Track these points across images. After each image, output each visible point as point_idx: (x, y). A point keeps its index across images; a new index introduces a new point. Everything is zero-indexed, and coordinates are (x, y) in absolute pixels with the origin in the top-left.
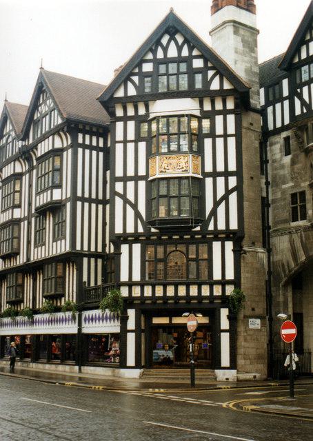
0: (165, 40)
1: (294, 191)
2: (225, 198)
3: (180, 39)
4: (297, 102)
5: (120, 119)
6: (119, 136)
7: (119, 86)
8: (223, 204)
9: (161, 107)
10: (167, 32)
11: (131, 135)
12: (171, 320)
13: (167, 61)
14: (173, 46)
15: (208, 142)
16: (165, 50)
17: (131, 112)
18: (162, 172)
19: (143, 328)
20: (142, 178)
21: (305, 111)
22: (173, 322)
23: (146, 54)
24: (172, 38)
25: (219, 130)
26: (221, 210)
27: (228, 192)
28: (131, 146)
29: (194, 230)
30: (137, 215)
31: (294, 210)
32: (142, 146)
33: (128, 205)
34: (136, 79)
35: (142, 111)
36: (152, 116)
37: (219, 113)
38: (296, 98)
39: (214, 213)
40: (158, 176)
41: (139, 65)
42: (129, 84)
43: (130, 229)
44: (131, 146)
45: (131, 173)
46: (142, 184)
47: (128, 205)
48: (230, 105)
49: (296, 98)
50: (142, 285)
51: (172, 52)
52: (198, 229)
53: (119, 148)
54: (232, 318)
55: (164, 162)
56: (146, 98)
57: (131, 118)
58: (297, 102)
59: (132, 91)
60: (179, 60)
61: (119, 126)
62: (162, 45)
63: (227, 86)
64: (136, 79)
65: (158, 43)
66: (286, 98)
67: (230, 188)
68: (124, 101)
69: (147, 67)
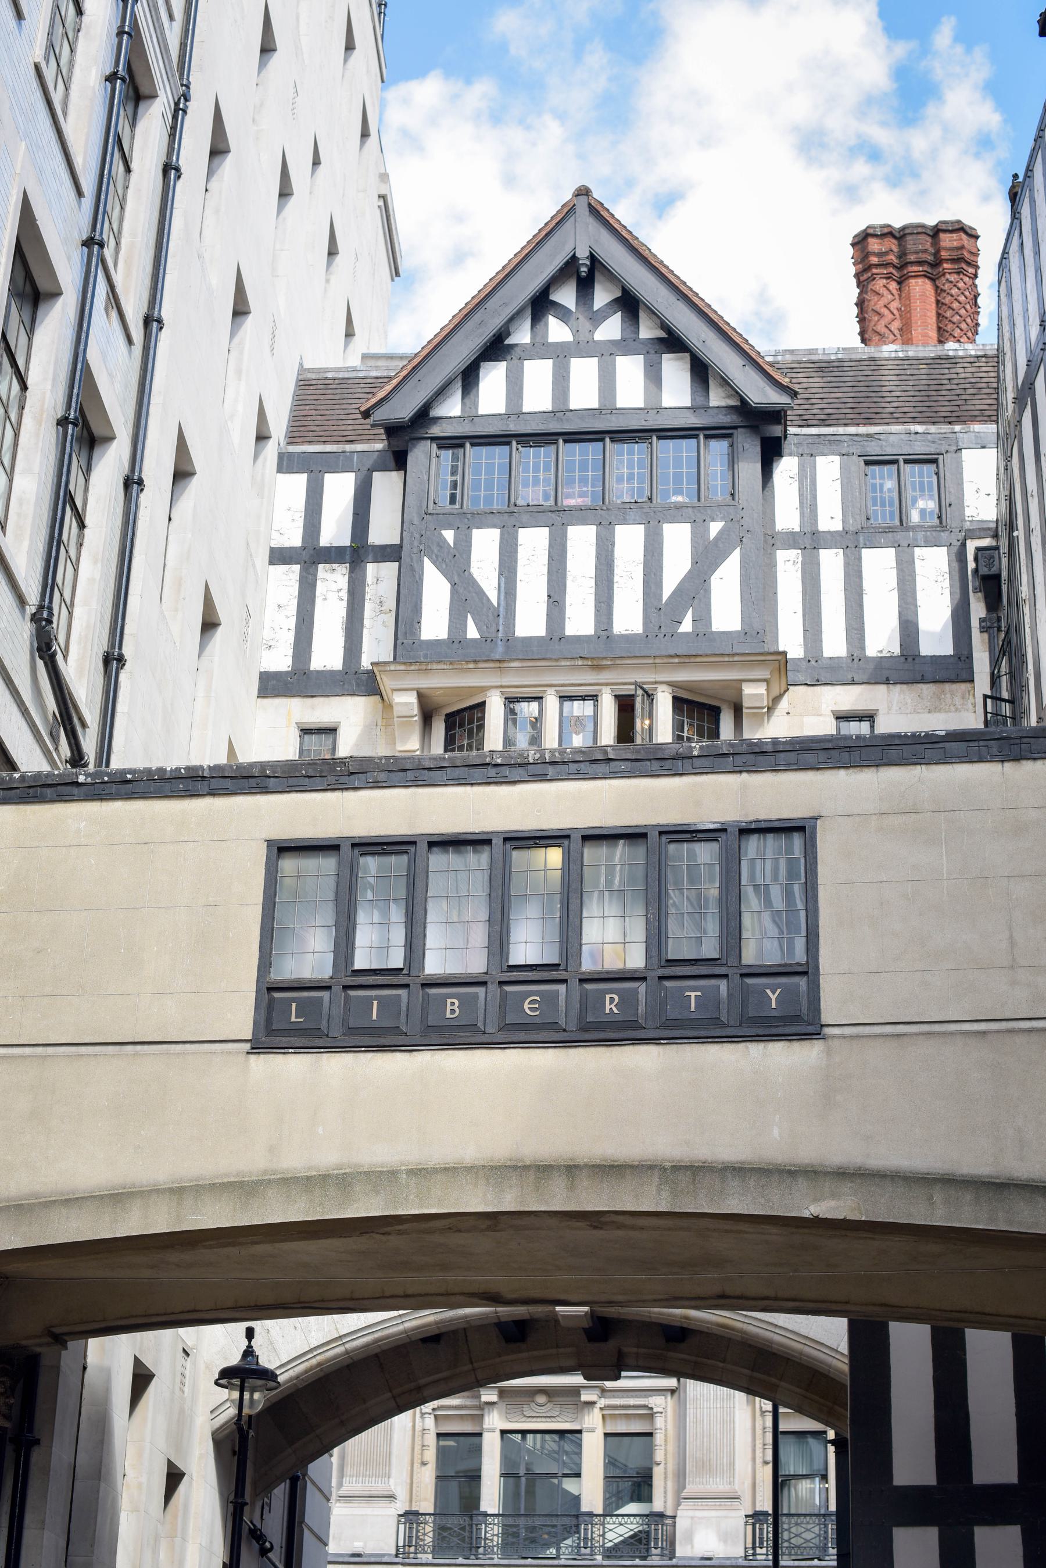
4: (436, 590)
21: (472, 632)
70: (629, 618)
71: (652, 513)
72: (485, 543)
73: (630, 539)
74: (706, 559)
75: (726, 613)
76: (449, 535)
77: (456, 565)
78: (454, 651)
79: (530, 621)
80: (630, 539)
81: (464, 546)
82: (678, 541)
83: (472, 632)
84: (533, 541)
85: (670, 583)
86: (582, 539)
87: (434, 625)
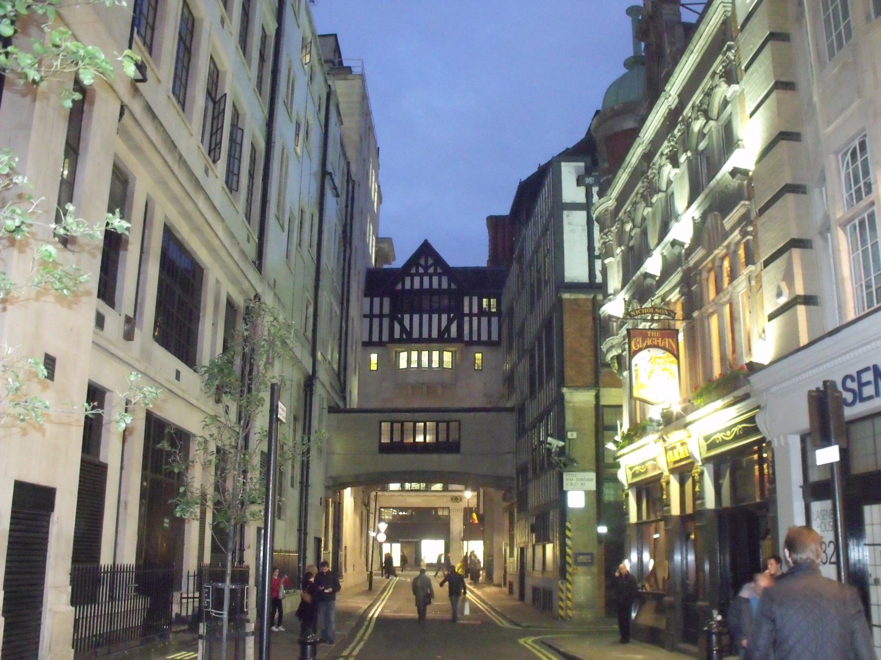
4: (397, 328)
21: (404, 337)
58: (397, 328)
71: (440, 312)
72: (407, 317)
73: (435, 317)
79: (416, 335)
80: (435, 317)
82: (444, 317)
83: (404, 337)
84: (416, 317)
85: (443, 328)
86: (426, 317)
87: (397, 335)
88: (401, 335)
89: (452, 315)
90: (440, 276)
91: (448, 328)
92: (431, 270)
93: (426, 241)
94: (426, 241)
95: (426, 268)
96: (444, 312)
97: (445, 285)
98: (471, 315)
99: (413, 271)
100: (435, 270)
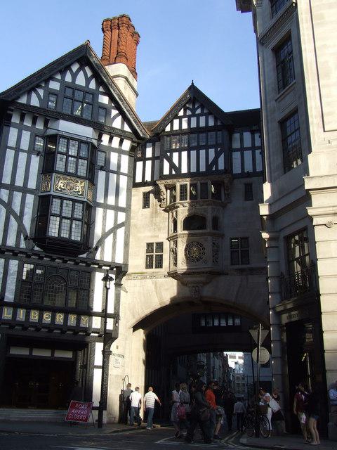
0: (75, 67)
1: (150, 241)
2: (114, 230)
3: (89, 73)
4: (166, 165)
5: (15, 126)
6: (12, 142)
7: (23, 94)
8: (111, 236)
9: (65, 126)
10: (78, 61)
11: (25, 145)
12: (53, 354)
13: (74, 87)
14: (81, 74)
15: (102, 175)
16: (74, 76)
17: (28, 123)
18: (57, 190)
19: (99, 347)
20: (31, 191)
21: (174, 172)
22: (55, 356)
23: (56, 73)
24: (81, 68)
25: (113, 167)
26: (109, 241)
27: (117, 227)
28: (23, 157)
29: (81, 256)
30: (21, 229)
31: (149, 258)
32: (36, 161)
33: (12, 218)
34: (41, 92)
35: (40, 126)
36: (50, 132)
37: (114, 150)
38: (165, 160)
39: (101, 242)
40: (52, 193)
41: (47, 81)
42: (34, 95)
43: (11, 242)
44: (23, 157)
45: (19, 182)
46: (30, 199)
47: (12, 218)
48: (127, 145)
49: (165, 160)
50: (15, 306)
51: (81, 80)
52: (84, 256)
53: (10, 154)
54: (106, 354)
55: (61, 181)
56: (48, 115)
57: (27, 128)
58: (166, 165)
59: (35, 101)
60: (85, 91)
61: (13, 133)
62: (71, 71)
63: (127, 128)
64: (41, 92)
65: (68, 68)
66: (149, 159)
67: (119, 222)
68: (26, 111)
69: (54, 85)
70: (203, 169)
71: (207, 148)
72: (176, 155)
73: (203, 152)
74: (217, 155)
75: (221, 166)
76: (169, 154)
77: (170, 160)
78: (170, 176)
80: (203, 152)
81: (171, 156)
82: (212, 152)
83: (174, 172)
87: (166, 171)
88: (171, 171)
89: (219, 149)
90: (207, 116)
91: (215, 161)
92: (198, 111)
93: (193, 89)
94: (193, 89)
95: (193, 110)
96: (211, 147)
97: (211, 123)
98: (242, 149)
99: (181, 113)
100: (202, 111)
